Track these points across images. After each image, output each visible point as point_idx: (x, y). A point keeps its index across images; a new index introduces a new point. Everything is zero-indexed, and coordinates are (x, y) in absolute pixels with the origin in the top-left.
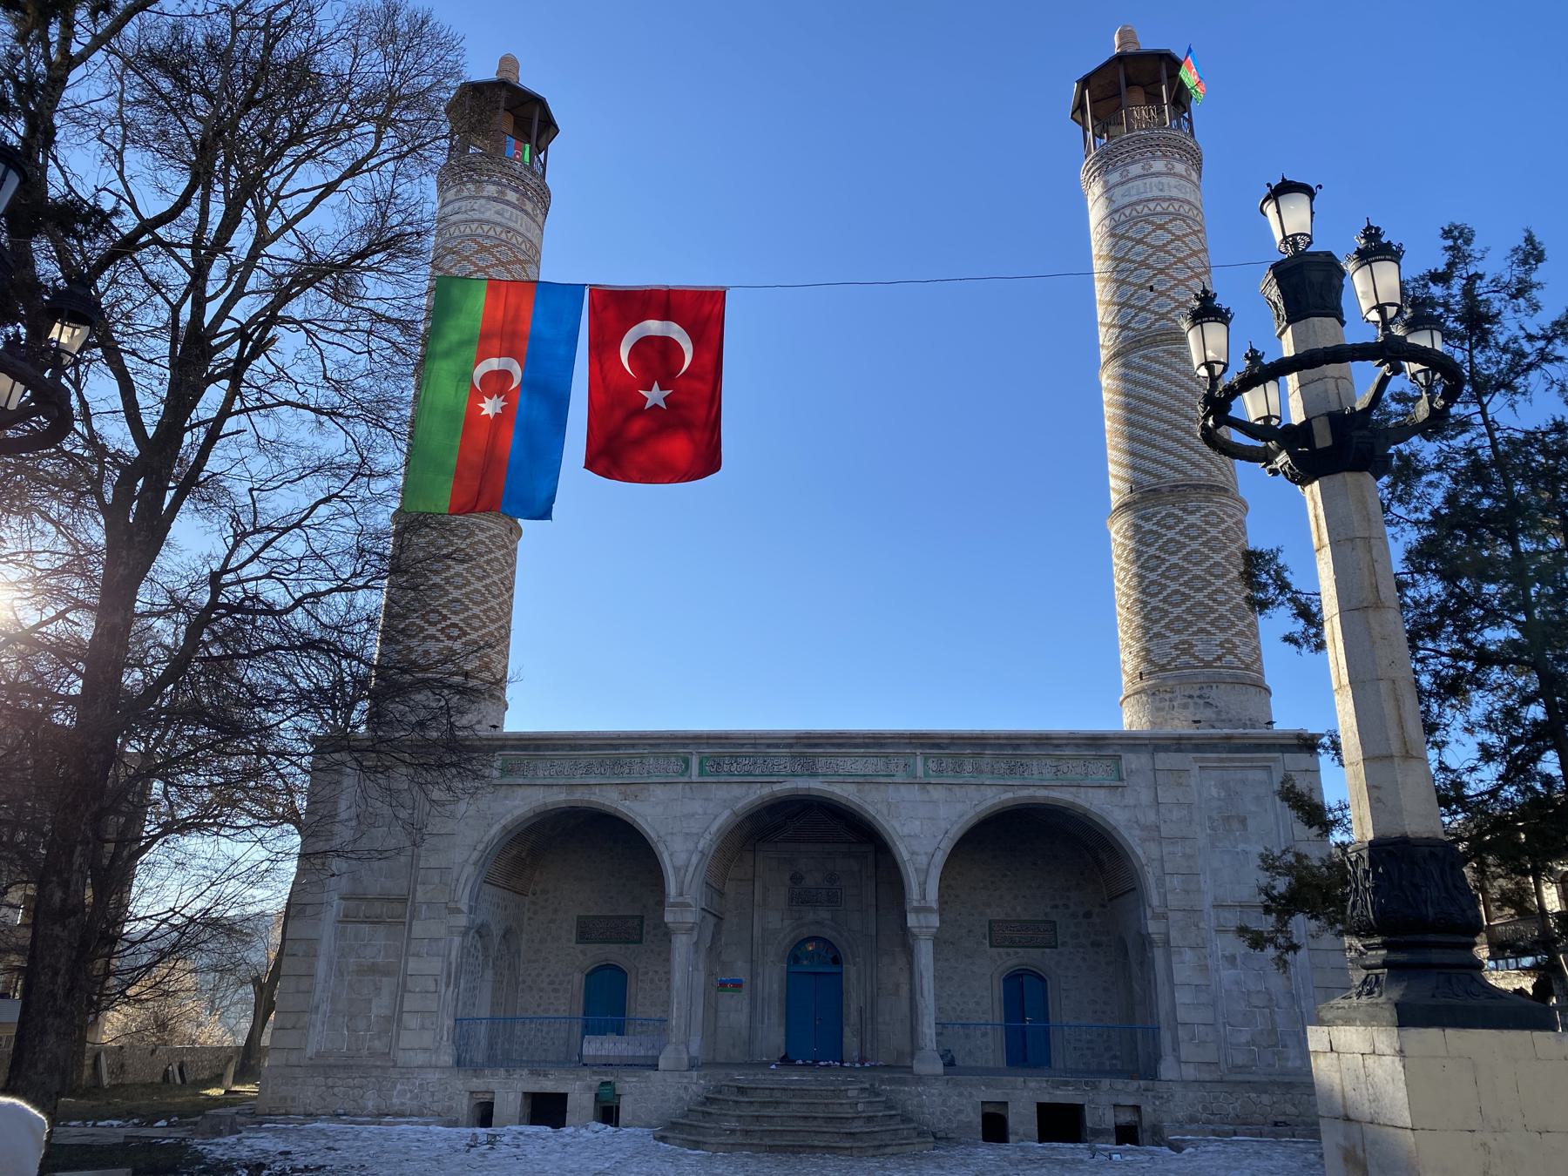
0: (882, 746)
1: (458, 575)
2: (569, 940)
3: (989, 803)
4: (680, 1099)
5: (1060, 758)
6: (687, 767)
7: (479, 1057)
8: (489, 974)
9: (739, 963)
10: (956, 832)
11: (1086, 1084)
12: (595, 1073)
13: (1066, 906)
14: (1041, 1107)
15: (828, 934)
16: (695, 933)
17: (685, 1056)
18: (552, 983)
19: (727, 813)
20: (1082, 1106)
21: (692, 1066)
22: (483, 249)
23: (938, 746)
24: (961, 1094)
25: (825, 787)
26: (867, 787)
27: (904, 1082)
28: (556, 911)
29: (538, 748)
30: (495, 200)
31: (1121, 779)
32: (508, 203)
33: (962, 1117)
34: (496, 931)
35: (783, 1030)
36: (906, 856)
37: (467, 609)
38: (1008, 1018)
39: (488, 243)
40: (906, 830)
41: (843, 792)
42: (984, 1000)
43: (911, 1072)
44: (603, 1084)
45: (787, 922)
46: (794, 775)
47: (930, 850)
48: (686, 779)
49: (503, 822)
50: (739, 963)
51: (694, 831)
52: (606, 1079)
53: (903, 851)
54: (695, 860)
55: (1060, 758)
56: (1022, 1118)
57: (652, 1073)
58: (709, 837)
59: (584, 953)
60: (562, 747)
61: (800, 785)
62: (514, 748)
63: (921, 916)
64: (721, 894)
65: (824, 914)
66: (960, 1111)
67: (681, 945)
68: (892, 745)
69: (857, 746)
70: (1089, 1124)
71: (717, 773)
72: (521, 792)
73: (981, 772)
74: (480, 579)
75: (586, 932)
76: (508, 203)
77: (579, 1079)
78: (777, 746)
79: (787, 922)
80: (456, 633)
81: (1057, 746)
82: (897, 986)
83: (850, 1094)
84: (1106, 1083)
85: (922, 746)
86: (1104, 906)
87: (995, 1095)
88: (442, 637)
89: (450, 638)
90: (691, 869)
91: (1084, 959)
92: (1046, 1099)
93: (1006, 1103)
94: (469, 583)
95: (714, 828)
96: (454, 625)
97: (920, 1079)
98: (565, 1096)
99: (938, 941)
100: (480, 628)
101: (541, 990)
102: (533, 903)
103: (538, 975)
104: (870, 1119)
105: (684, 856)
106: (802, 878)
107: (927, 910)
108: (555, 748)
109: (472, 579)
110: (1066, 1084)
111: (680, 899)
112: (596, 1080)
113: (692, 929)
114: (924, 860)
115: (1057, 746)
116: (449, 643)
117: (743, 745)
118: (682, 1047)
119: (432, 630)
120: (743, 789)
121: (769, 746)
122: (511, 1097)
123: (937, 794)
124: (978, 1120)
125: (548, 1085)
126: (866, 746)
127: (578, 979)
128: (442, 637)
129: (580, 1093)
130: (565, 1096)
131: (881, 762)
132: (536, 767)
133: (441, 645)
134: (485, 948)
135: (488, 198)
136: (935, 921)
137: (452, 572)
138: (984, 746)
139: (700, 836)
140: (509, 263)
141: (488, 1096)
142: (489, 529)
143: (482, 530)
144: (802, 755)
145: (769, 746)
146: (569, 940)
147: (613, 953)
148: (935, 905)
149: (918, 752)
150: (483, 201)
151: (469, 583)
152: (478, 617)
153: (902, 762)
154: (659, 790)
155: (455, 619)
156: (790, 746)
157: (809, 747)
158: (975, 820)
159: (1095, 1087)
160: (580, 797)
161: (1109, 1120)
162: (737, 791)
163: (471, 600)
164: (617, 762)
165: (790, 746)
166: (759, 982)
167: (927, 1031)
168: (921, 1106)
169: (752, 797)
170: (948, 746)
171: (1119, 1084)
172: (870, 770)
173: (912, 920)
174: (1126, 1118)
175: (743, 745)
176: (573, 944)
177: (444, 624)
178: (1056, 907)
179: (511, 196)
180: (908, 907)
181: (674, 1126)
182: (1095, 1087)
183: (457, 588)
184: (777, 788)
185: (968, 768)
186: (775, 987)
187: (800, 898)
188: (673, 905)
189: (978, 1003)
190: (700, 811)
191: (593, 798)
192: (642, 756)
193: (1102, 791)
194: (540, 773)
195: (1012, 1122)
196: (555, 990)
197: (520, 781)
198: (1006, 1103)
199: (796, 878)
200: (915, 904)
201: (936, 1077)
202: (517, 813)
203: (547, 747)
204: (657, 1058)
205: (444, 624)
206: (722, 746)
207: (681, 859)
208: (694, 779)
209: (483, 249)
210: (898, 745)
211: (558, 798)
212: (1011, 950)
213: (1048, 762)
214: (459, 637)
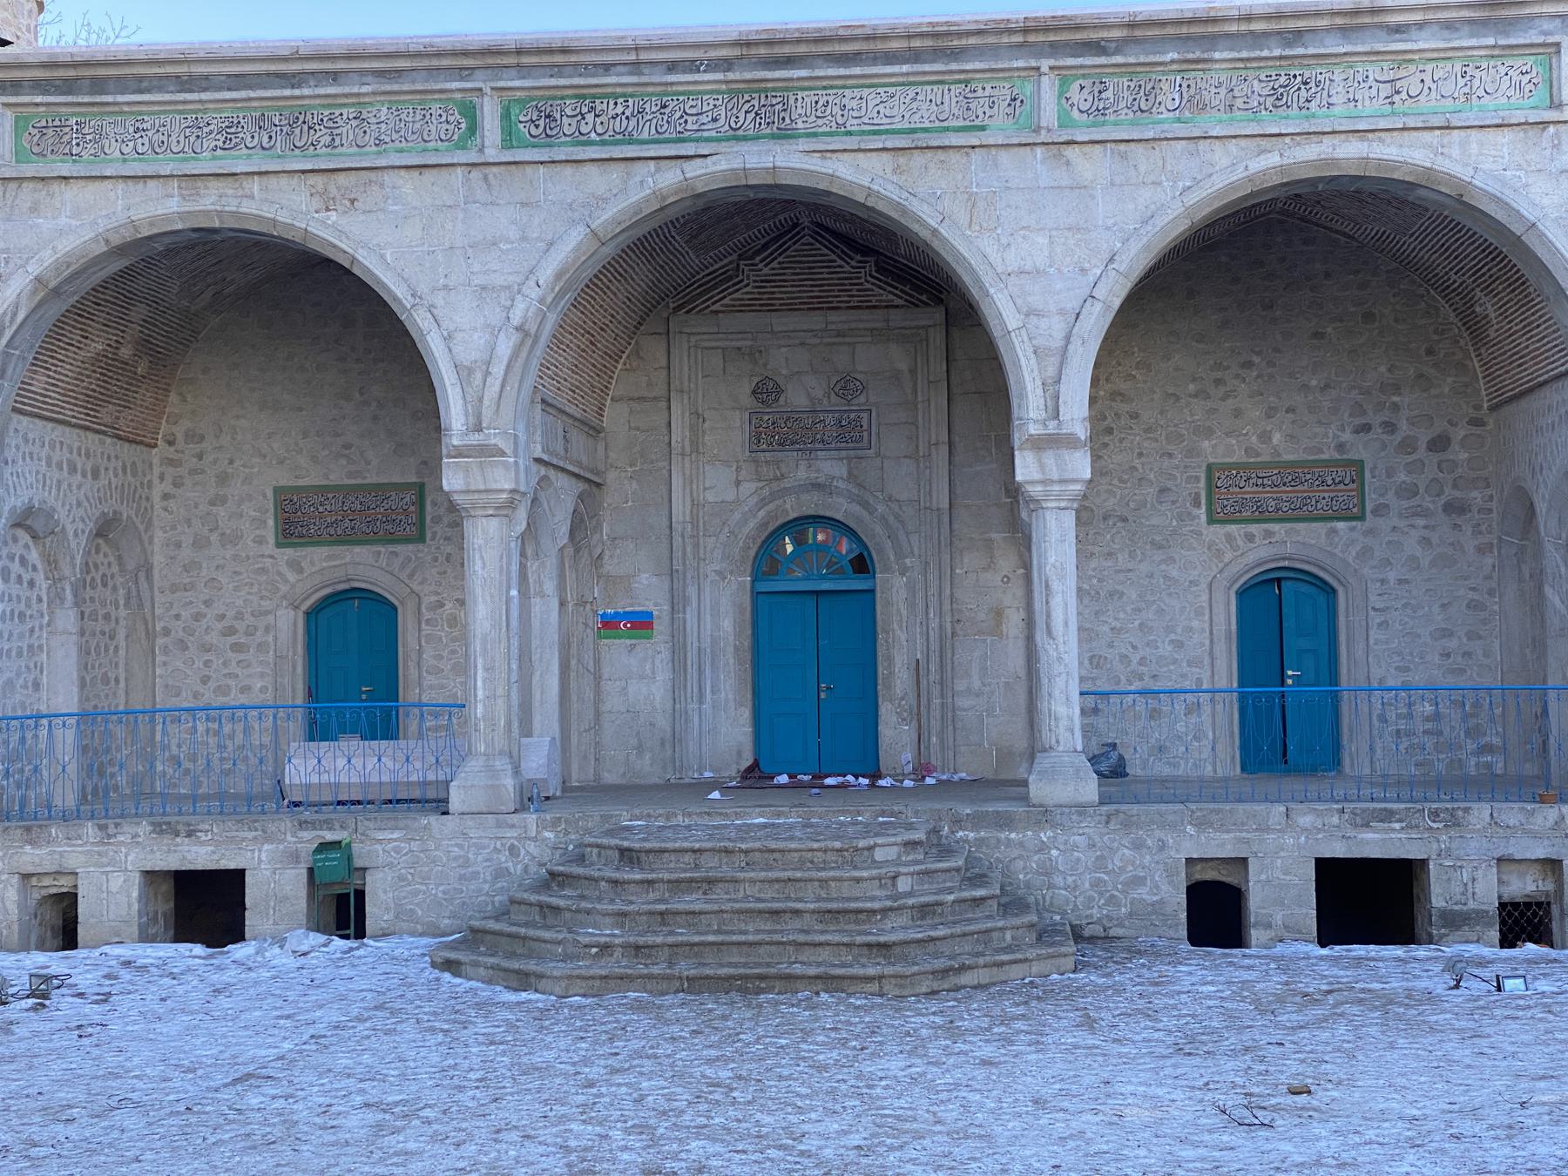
0: (956, 54)
2: (260, 541)
3: (1219, 182)
4: (500, 873)
5: (1402, 59)
6: (473, 129)
7: (66, 797)
8: (67, 619)
9: (644, 578)
10: (1135, 258)
11: (1435, 815)
12: (303, 825)
13: (1390, 427)
14: (1322, 864)
15: (840, 508)
16: (522, 514)
17: (509, 782)
18: (230, 631)
19: (576, 235)
20: (1424, 863)
21: (530, 798)
23: (1097, 48)
24: (1138, 846)
25: (814, 164)
26: (919, 159)
27: (1004, 821)
28: (223, 479)
29: (98, 85)
31: (1555, 105)
33: (1143, 893)
34: (75, 524)
35: (746, 714)
36: (1012, 321)
38: (1248, 672)
40: (1012, 260)
41: (861, 175)
42: (1196, 639)
43: (1025, 799)
44: (324, 847)
45: (748, 487)
46: (736, 136)
47: (1073, 304)
48: (472, 157)
49: (34, 269)
50: (644, 578)
51: (499, 280)
52: (330, 836)
53: (1004, 309)
54: (505, 348)
55: (1402, 59)
56: (1281, 892)
57: (434, 820)
58: (535, 293)
59: (295, 566)
60: (159, 83)
61: (753, 162)
62: (39, 86)
63: (1049, 458)
64: (595, 431)
65: (831, 467)
66: (1138, 881)
67: (488, 545)
68: (980, 52)
69: (890, 58)
70: (1438, 901)
71: (548, 139)
72: (70, 193)
73: (1204, 107)
75: (295, 522)
77: (268, 840)
78: (693, 66)
79: (748, 487)
81: (1398, 29)
82: (998, 613)
83: (879, 855)
84: (1480, 813)
85: (1055, 49)
86: (1477, 422)
87: (1219, 844)
90: (498, 370)
91: (1426, 541)
92: (1338, 850)
93: (1244, 860)
95: (546, 273)
97: (1045, 815)
98: (240, 874)
99: (1086, 515)
101: (206, 648)
102: (171, 462)
103: (197, 617)
104: (924, 911)
105: (479, 339)
106: (779, 391)
107: (1070, 442)
108: (140, 84)
110: (1388, 816)
111: (475, 439)
112: (308, 840)
113: (511, 505)
114: (1055, 328)
115: (1398, 29)
117: (607, 68)
118: (502, 764)
120: (615, 173)
121: (672, 66)
122: (117, 882)
123: (1089, 166)
124: (1178, 900)
125: (200, 855)
126: (915, 56)
127: (288, 625)
129: (274, 873)
130: (239, 875)
131: (951, 98)
132: (100, 134)
134: (51, 563)
136: (1080, 465)
138: (1213, 40)
139: (513, 292)
141: (64, 885)
144: (758, 88)
145: (672, 66)
146: (260, 541)
147: (364, 565)
148: (1082, 432)
149: (1045, 64)
153: (1004, 93)
154: (407, 184)
156: (727, 64)
157: (768, 67)
158: (1183, 227)
159: (1454, 822)
160: (217, 205)
161: (1487, 891)
162: (598, 181)
164: (297, 120)
165: (727, 64)
166: (690, 616)
167: (1061, 709)
168: (1047, 871)
169: (636, 196)
170: (1121, 46)
171: (1512, 814)
172: (925, 115)
173: (1026, 468)
174: (1525, 886)
175: (607, 68)
176: (270, 547)
178: (1366, 428)
180: (1017, 439)
181: (475, 937)
182: (1454, 822)
184: (694, 169)
185: (1169, 95)
186: (727, 624)
187: (777, 432)
188: (459, 453)
189: (1179, 645)
190: (513, 233)
191: (248, 207)
192: (359, 101)
193: (1506, 136)
194: (113, 150)
195: (1256, 902)
196: (237, 648)
197: (65, 169)
198: (1244, 860)
199: (766, 392)
200: (1033, 429)
201: (1081, 808)
202: (67, 245)
203: (123, 85)
204: (447, 783)
206: (559, 70)
207: (471, 348)
208: (492, 154)
210: (994, 51)
211: (161, 208)
212: (1254, 528)
213: (1374, 72)
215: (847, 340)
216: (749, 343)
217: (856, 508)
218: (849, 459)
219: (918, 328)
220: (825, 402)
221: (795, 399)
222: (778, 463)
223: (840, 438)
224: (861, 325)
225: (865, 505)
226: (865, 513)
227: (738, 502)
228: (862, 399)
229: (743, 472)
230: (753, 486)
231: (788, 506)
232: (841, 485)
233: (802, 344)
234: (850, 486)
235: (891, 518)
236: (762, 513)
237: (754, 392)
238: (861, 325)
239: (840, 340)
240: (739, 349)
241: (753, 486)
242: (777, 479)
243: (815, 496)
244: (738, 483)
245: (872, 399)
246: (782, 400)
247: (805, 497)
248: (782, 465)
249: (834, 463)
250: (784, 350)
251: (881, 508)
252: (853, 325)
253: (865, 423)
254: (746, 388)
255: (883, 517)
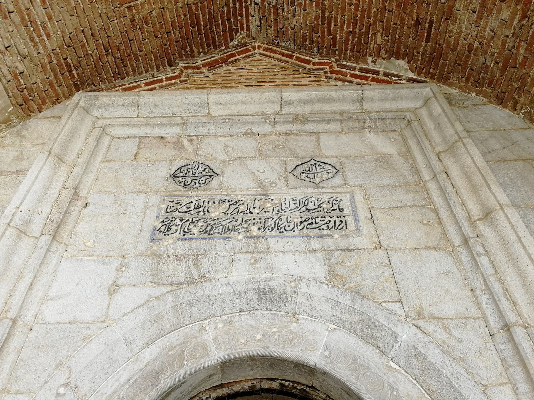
65: (292, 260)
106: (211, 173)
215: (309, 127)
216: (176, 130)
217: (354, 344)
218: (328, 252)
219: (402, 111)
220: (281, 184)
221: (236, 182)
222: (197, 258)
223: (308, 224)
224: (327, 108)
225: (368, 331)
226: (370, 352)
227: (105, 321)
228: (338, 180)
229: (130, 273)
230: (140, 294)
231: (209, 337)
232: (320, 292)
233: (246, 134)
234: (334, 294)
235: (435, 356)
236: (150, 354)
237: (174, 176)
238: (327, 108)
239: (296, 127)
240: (161, 138)
241: (140, 294)
242: (191, 282)
243: (264, 318)
244: (114, 288)
245: (351, 181)
246: (215, 183)
247: (244, 321)
248: (205, 262)
249: (299, 257)
250: (223, 139)
251: (406, 334)
252: (316, 107)
253: (346, 205)
254: (165, 171)
255: (416, 353)
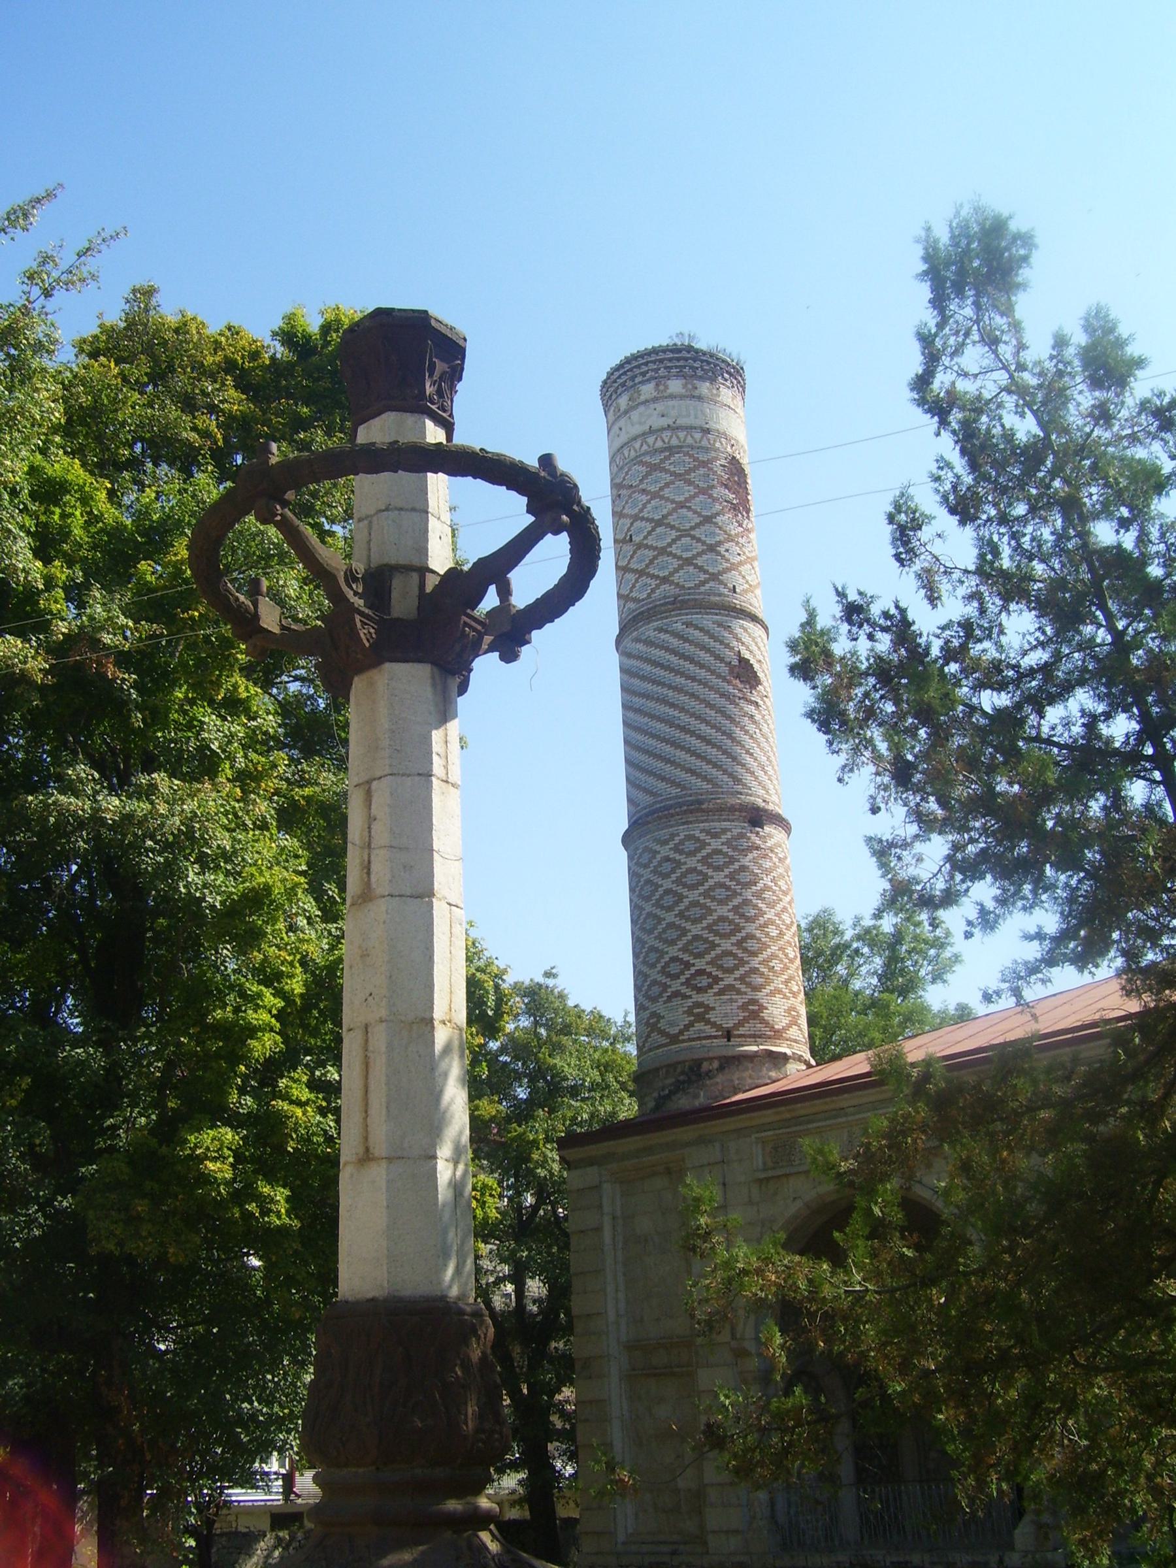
1: (695, 904)
22: (653, 468)
30: (655, 400)
32: (672, 397)
37: (714, 946)
39: (655, 460)
74: (722, 902)
76: (672, 397)
80: (704, 981)
88: (688, 992)
89: (700, 990)
94: (710, 911)
96: (700, 972)
100: (736, 967)
109: (713, 905)
116: (697, 998)
119: (676, 985)
128: (688, 992)
133: (689, 1002)
135: (646, 402)
137: (686, 902)
140: (688, 472)
142: (724, 831)
143: (715, 836)
150: (642, 409)
151: (710, 911)
152: (730, 953)
155: (700, 964)
163: (717, 933)
177: (687, 974)
179: (675, 386)
183: (695, 921)
197: (787, 1170)
205: (687, 974)
209: (653, 468)
214: (710, 986)
